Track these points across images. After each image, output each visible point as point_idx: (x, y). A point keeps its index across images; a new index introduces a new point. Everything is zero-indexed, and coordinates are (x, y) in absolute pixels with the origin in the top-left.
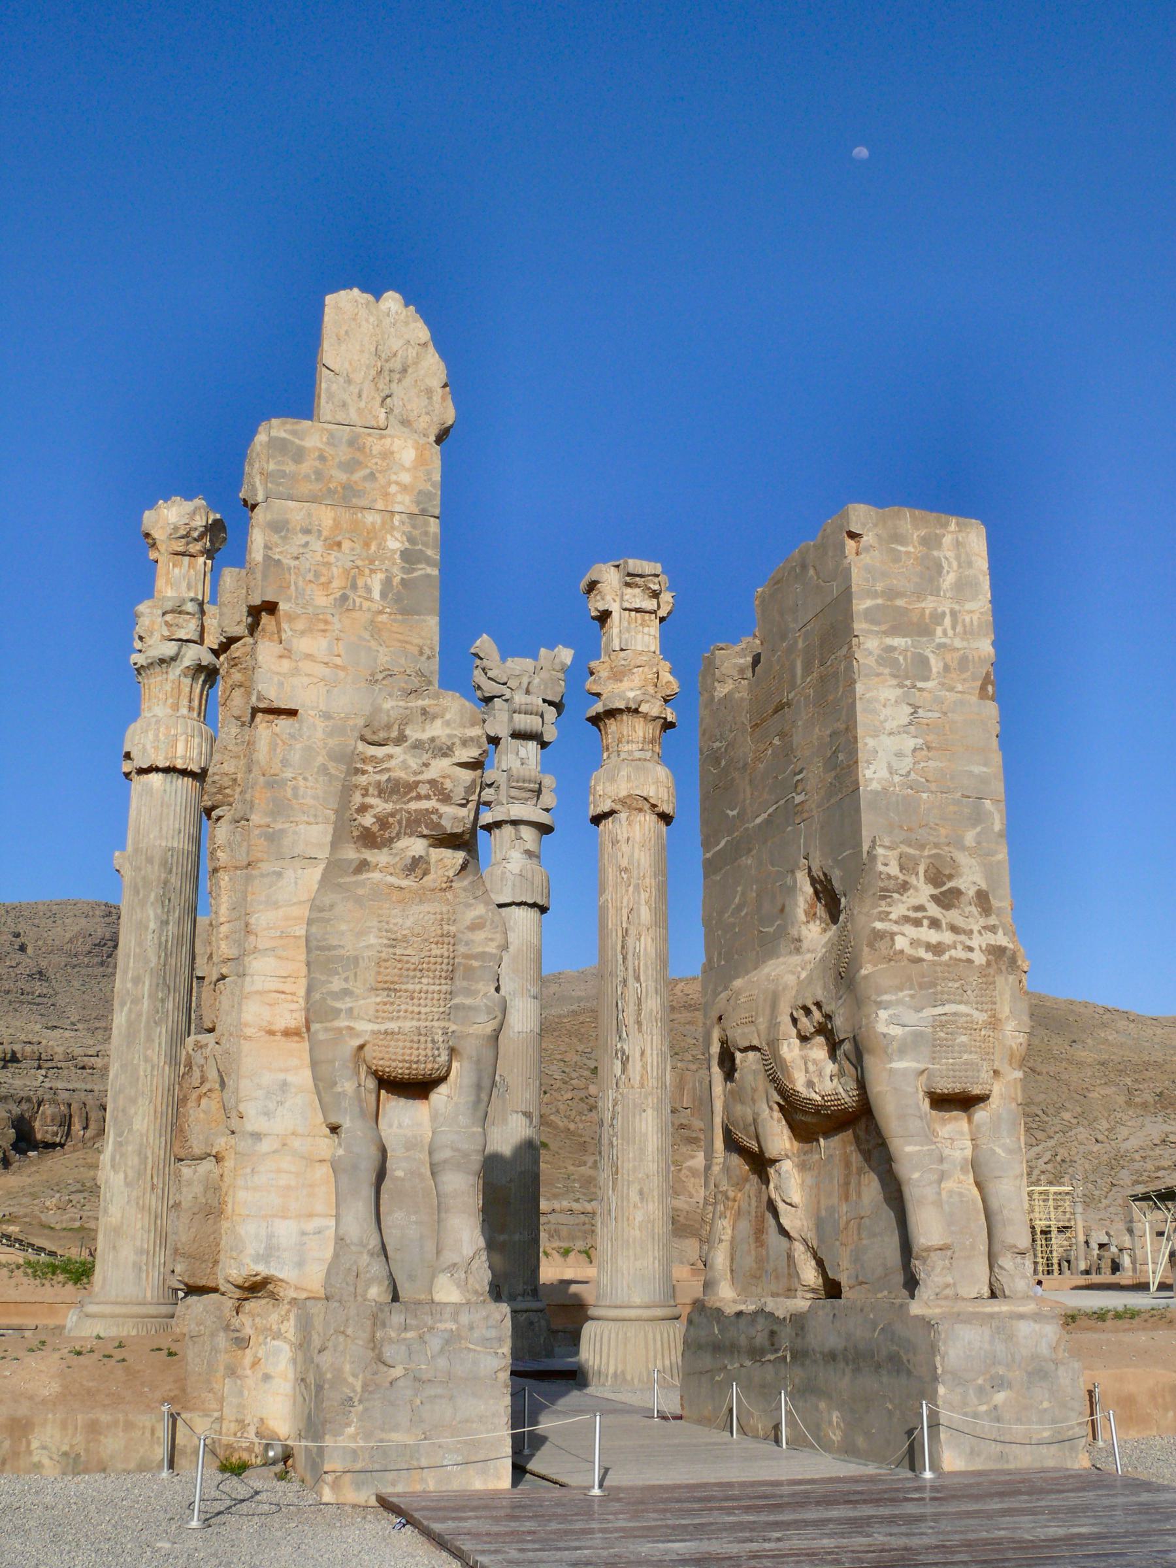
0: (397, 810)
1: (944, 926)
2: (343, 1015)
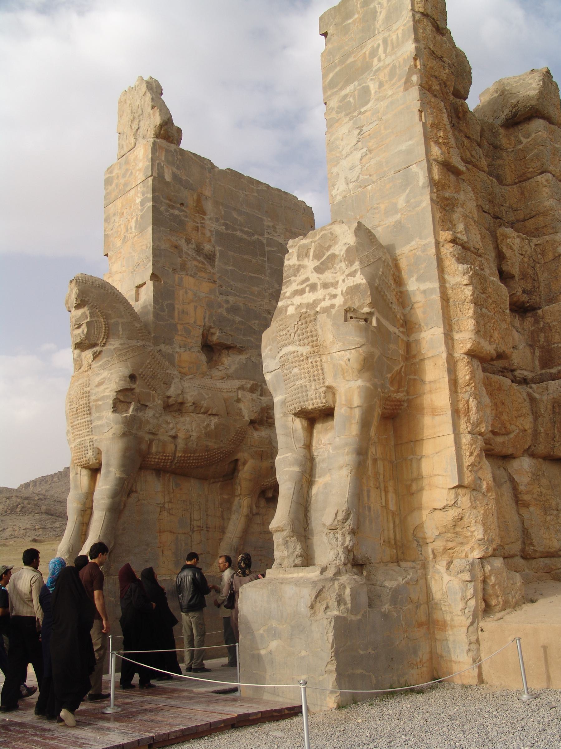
1: (319, 287)
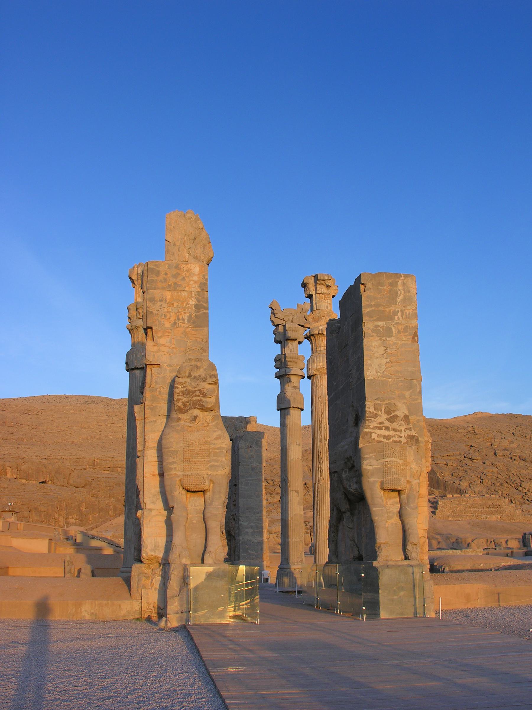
0: (189, 400)
1: (391, 429)
2: (173, 470)
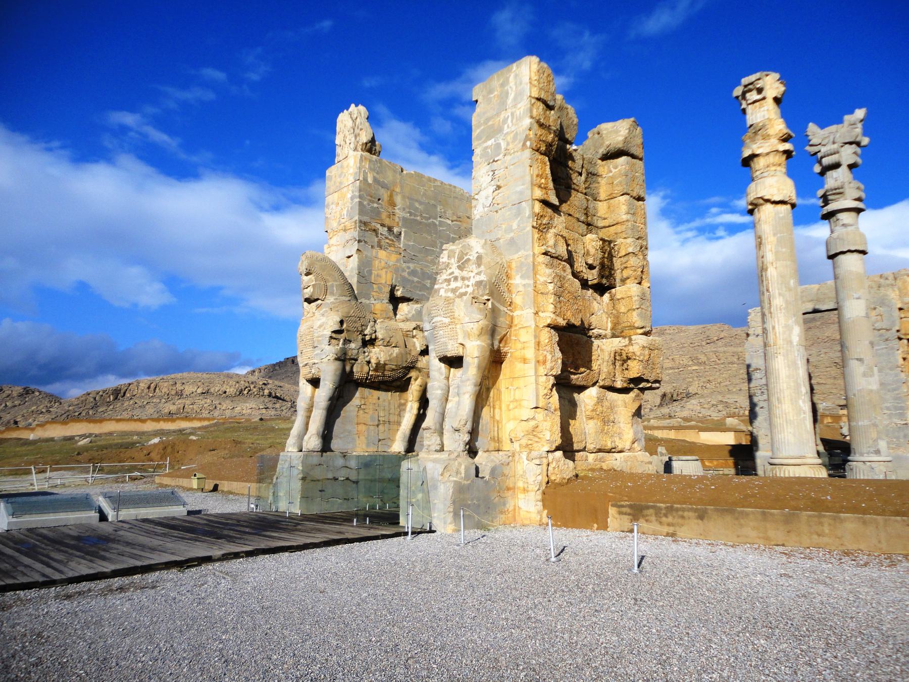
1: (459, 279)
